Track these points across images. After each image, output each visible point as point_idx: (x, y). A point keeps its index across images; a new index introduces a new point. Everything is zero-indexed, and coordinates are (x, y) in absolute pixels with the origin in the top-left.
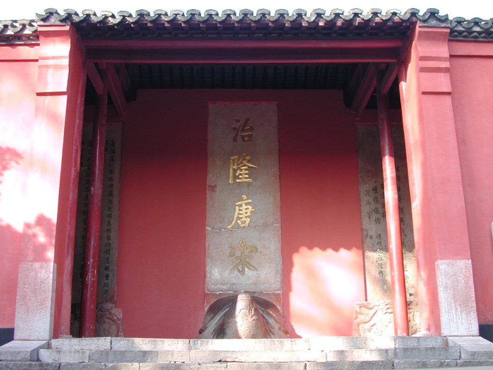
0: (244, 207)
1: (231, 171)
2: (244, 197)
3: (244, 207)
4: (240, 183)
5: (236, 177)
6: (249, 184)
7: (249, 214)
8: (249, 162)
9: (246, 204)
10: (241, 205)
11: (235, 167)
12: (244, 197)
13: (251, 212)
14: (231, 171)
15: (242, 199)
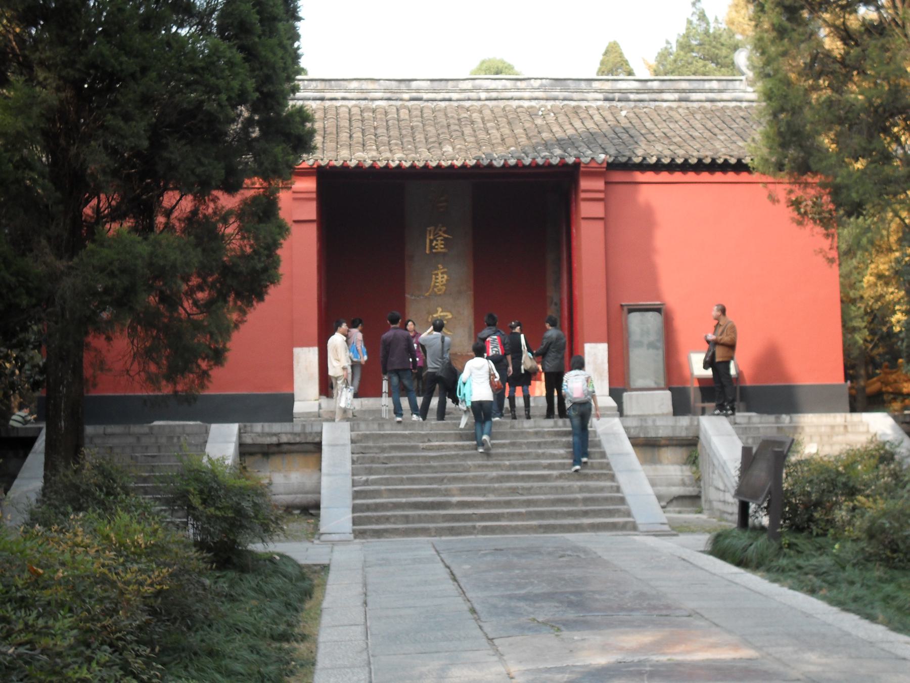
0: (440, 275)
1: (428, 241)
2: (440, 266)
3: (440, 275)
4: (436, 253)
5: (432, 248)
6: (444, 254)
7: (444, 282)
8: (445, 232)
9: (442, 273)
10: (437, 274)
11: (432, 237)
12: (440, 266)
13: (447, 280)
14: (428, 241)
15: (438, 269)
